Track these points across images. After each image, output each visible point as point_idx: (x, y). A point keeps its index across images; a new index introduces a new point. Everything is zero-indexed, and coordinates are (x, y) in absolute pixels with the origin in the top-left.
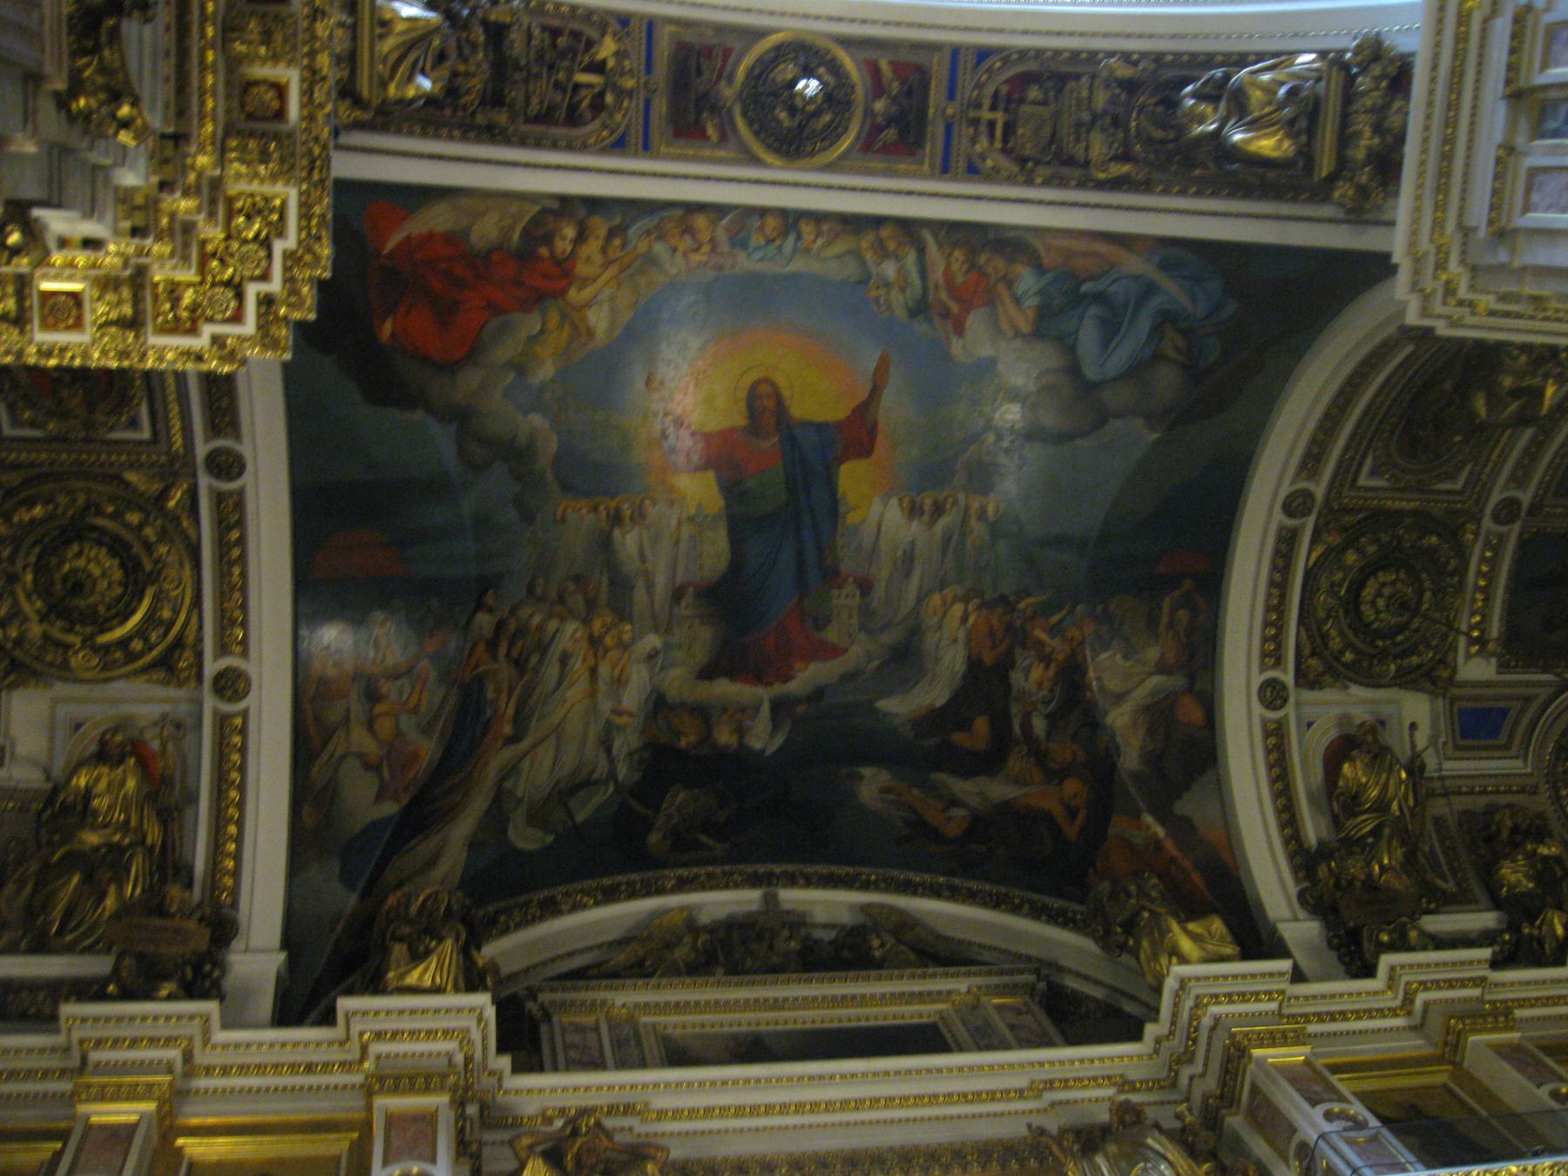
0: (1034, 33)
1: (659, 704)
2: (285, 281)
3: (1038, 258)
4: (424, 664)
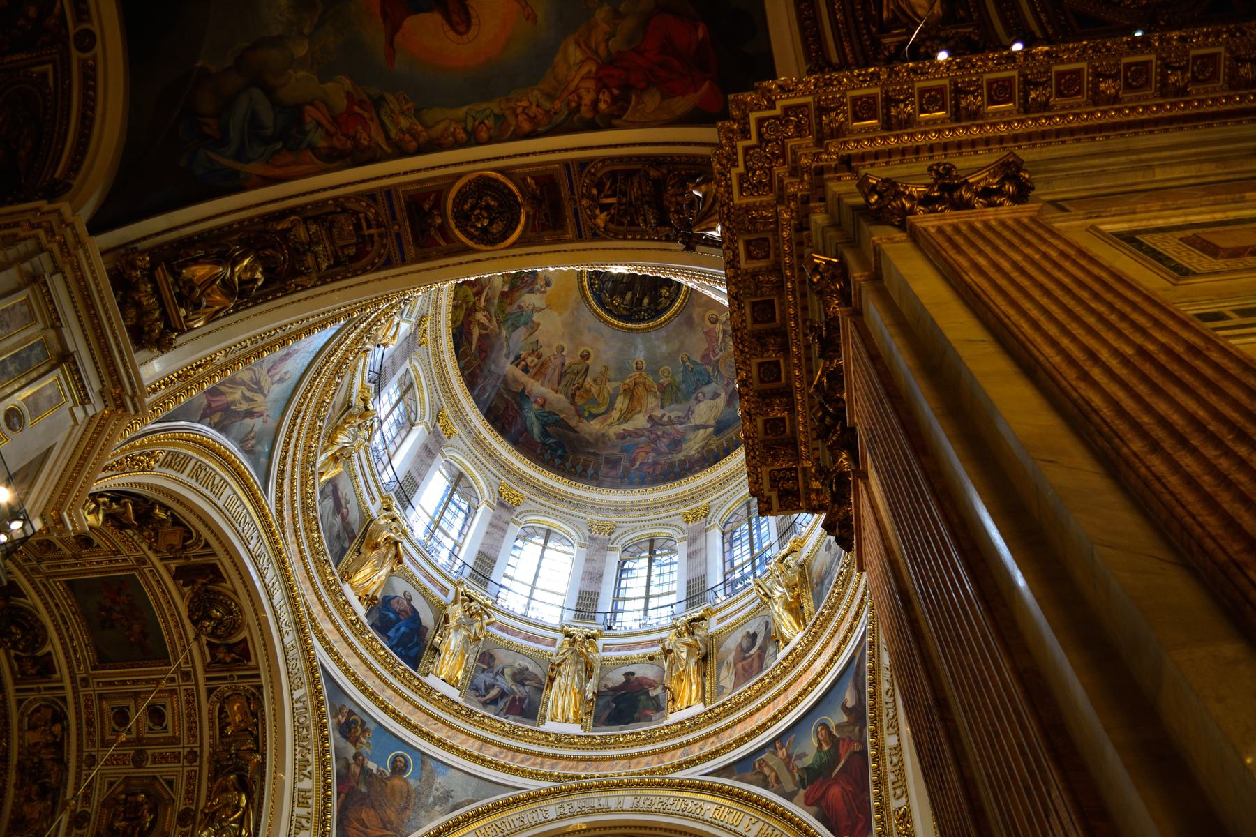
2: (735, 147)
3: (314, 154)
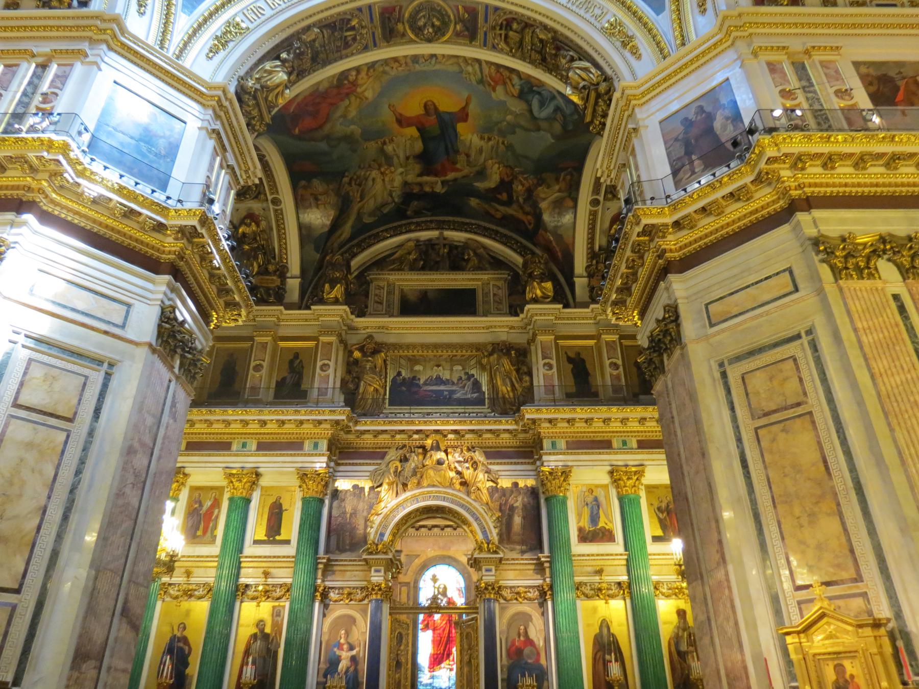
0: (516, 5)
1: (406, 184)
4: (330, 192)
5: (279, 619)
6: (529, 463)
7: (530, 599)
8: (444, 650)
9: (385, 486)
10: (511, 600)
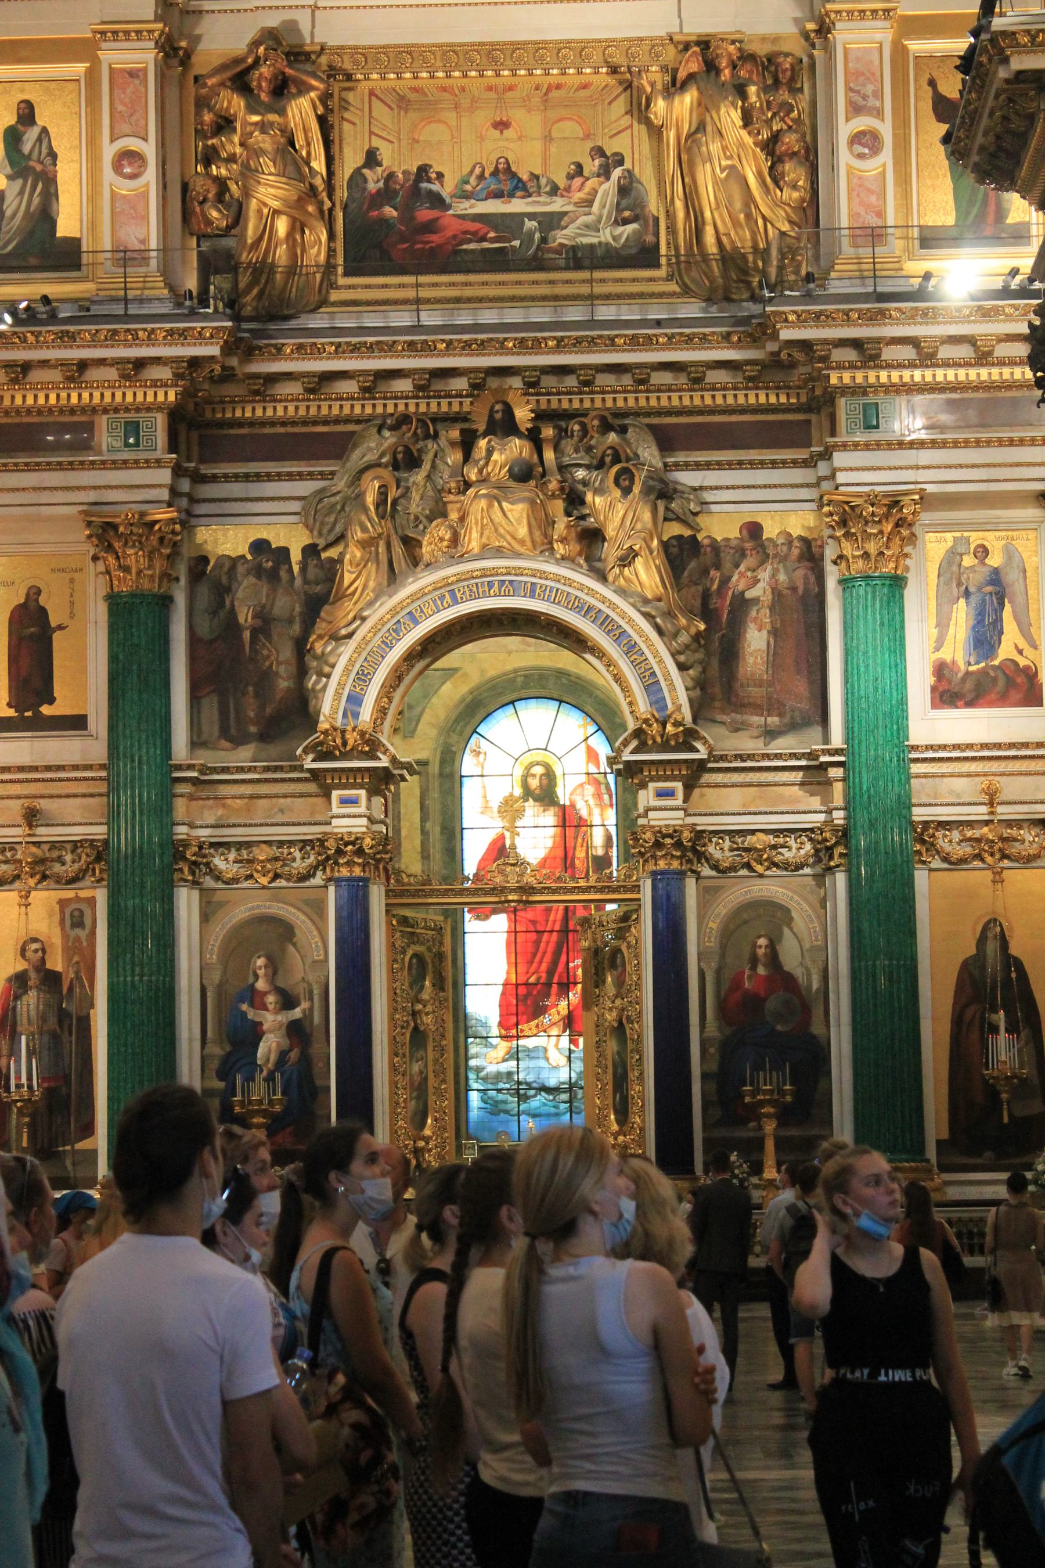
5: (83, 934)
6: (795, 463)
7: (786, 866)
8: (551, 972)
9: (354, 553)
10: (733, 868)
